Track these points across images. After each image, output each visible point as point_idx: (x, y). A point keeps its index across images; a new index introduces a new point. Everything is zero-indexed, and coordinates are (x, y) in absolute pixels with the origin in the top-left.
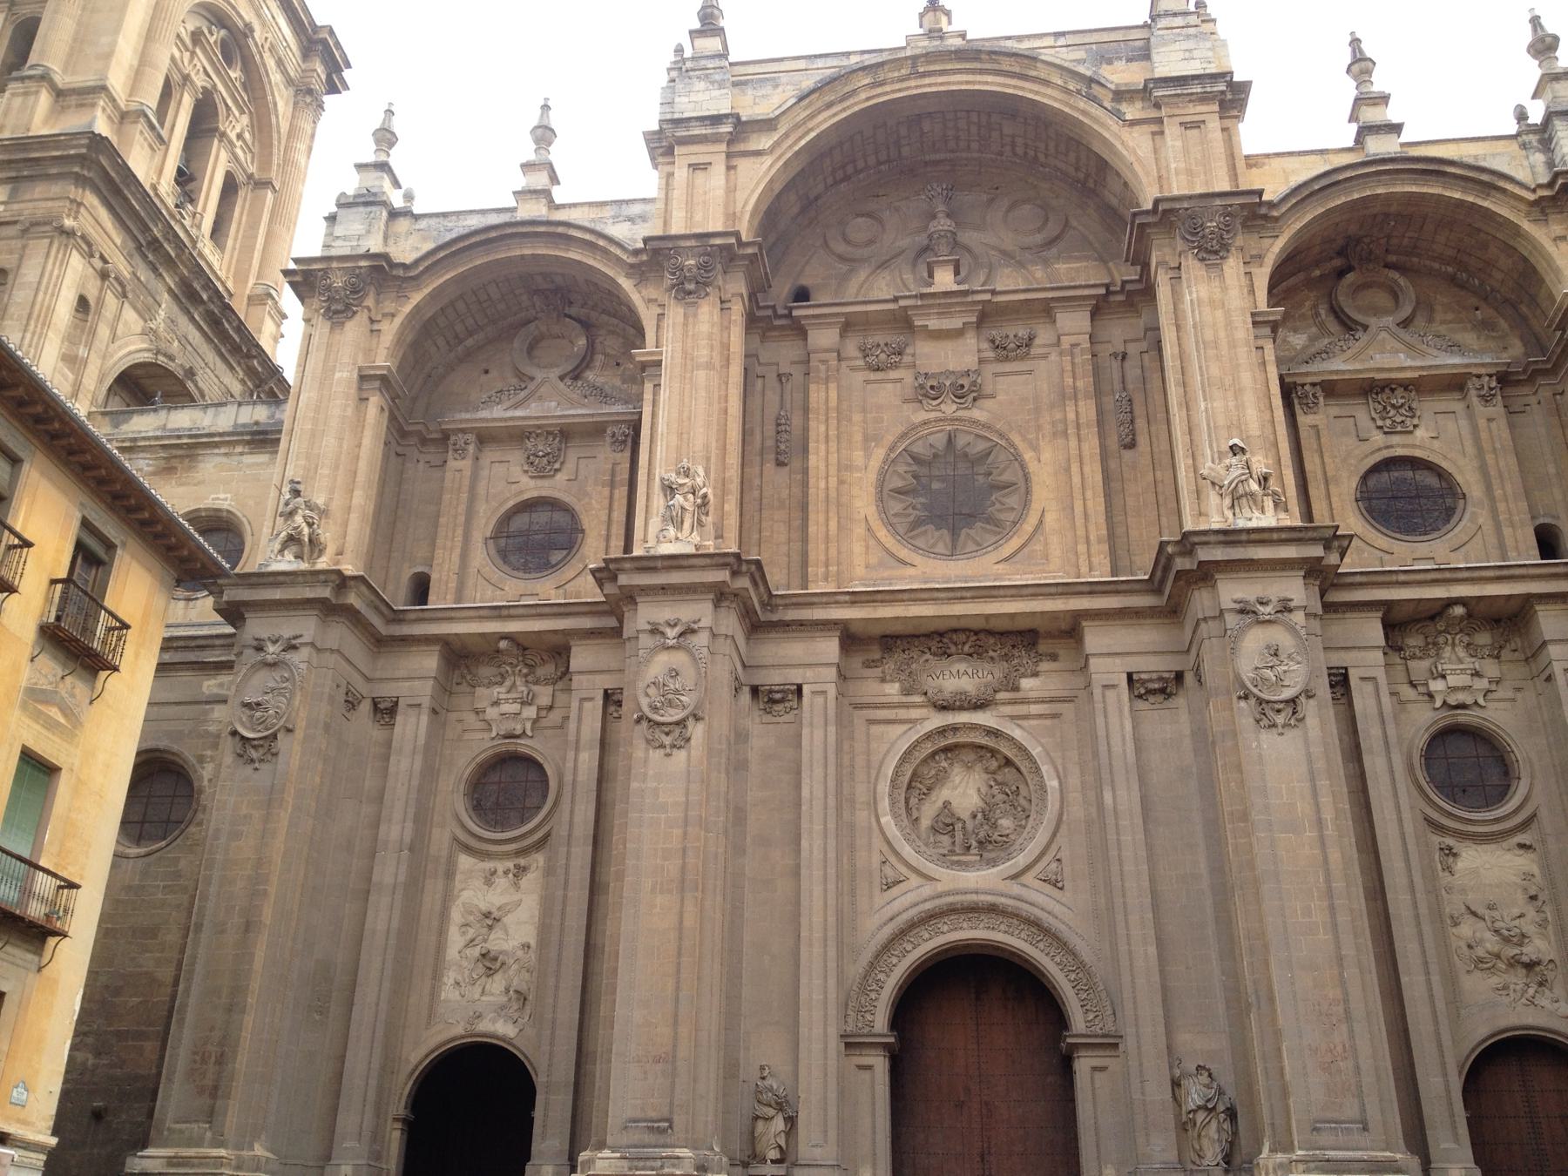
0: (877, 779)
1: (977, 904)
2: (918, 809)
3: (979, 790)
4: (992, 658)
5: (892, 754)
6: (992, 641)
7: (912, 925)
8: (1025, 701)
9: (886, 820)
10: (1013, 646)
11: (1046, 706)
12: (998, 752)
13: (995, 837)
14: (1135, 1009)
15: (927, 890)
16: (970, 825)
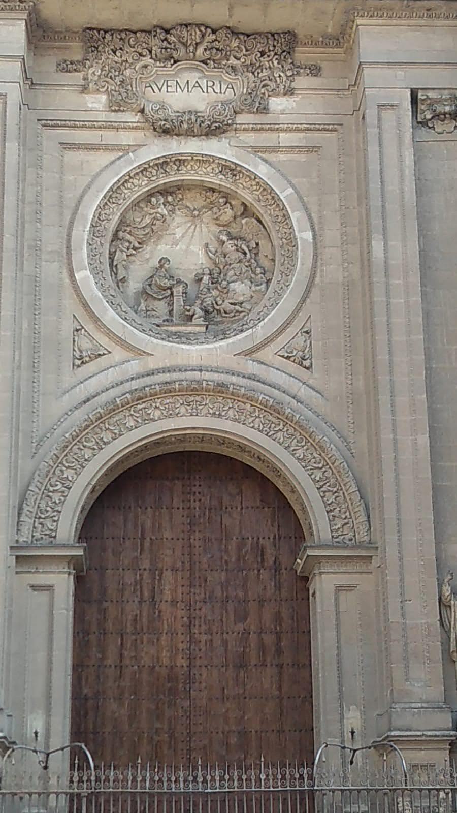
0: (71, 223)
1: (199, 382)
2: (126, 268)
3: (207, 245)
4: (232, 67)
5: (93, 188)
6: (235, 43)
7: (113, 409)
8: (274, 128)
9: (83, 275)
10: (263, 54)
11: (302, 135)
12: (235, 195)
13: (226, 306)
14: (398, 511)
15: (135, 366)
16: (192, 290)
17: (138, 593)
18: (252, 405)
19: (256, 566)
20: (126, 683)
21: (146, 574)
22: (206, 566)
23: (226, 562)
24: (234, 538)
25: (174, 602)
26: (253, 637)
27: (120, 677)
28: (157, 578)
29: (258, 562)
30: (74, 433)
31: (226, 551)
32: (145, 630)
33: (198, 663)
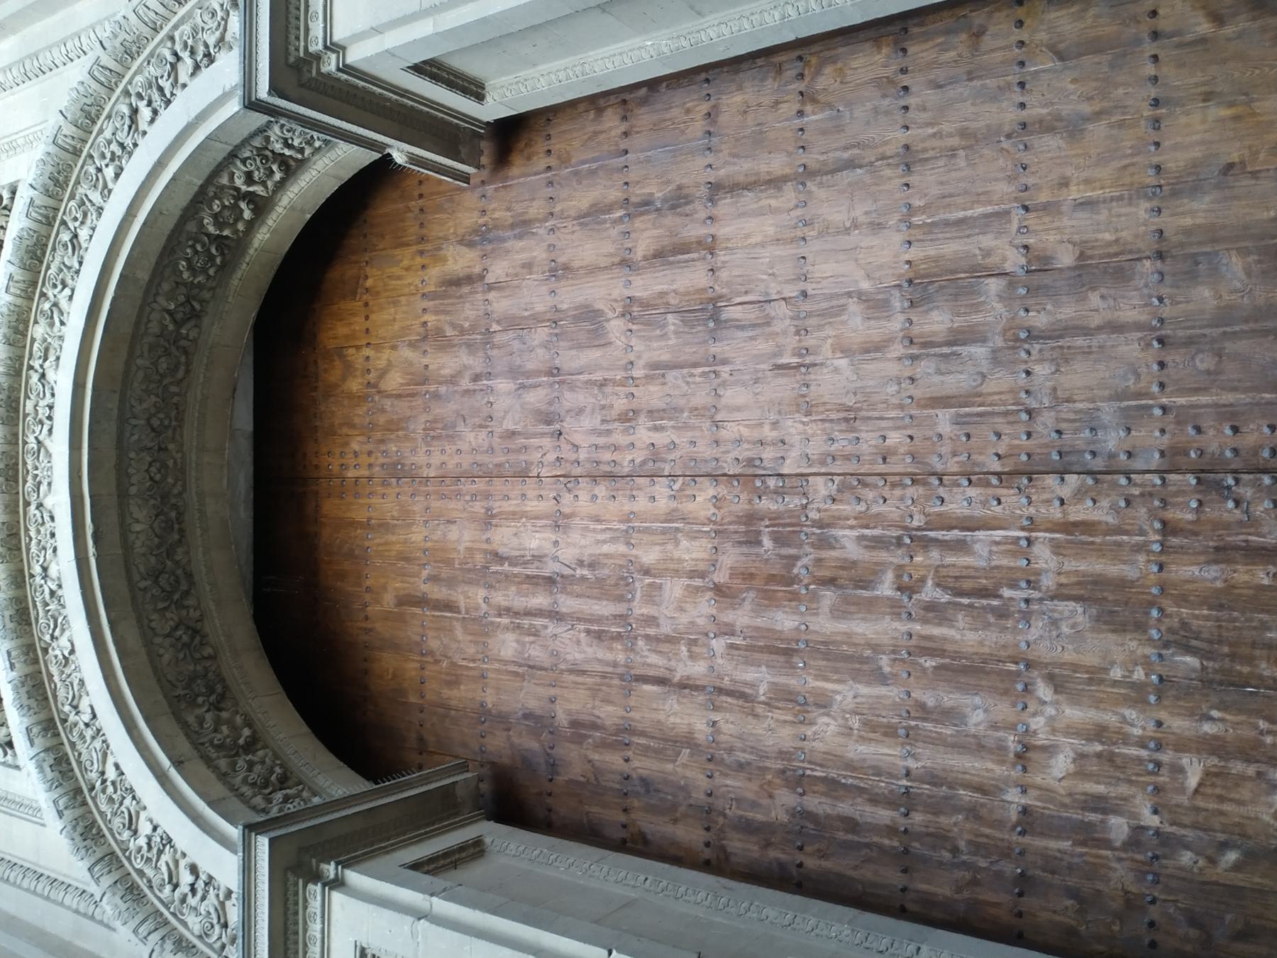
17: (539, 622)
18: (36, 322)
19: (480, 297)
20: (760, 677)
21: (499, 598)
22: (483, 434)
23: (476, 378)
24: (425, 361)
25: (560, 522)
26: (646, 285)
27: (742, 696)
28: (506, 567)
29: (471, 293)
30: (62, 802)
31: (452, 380)
32: (620, 609)
33: (704, 450)
